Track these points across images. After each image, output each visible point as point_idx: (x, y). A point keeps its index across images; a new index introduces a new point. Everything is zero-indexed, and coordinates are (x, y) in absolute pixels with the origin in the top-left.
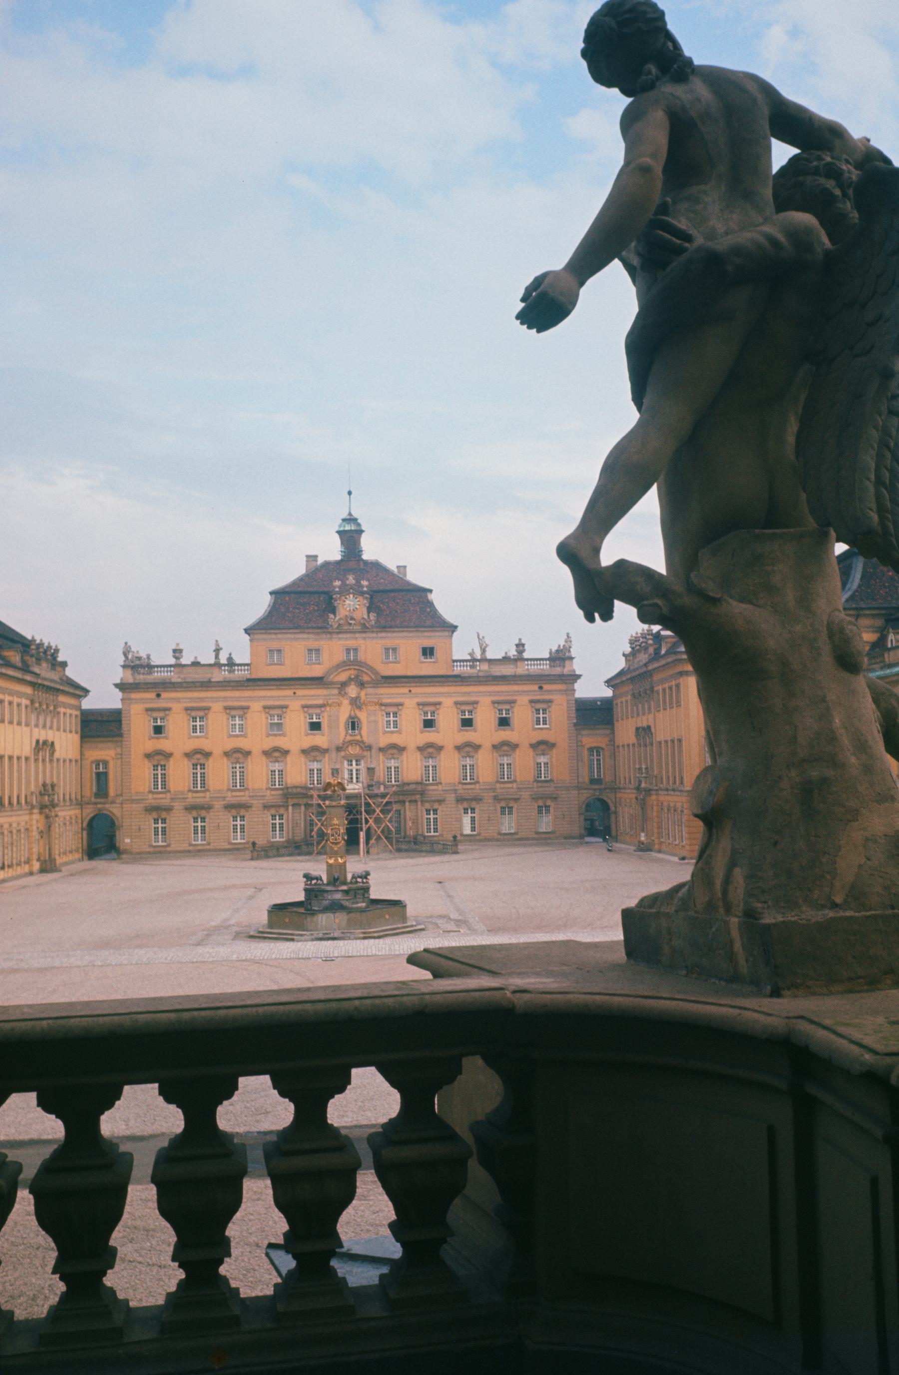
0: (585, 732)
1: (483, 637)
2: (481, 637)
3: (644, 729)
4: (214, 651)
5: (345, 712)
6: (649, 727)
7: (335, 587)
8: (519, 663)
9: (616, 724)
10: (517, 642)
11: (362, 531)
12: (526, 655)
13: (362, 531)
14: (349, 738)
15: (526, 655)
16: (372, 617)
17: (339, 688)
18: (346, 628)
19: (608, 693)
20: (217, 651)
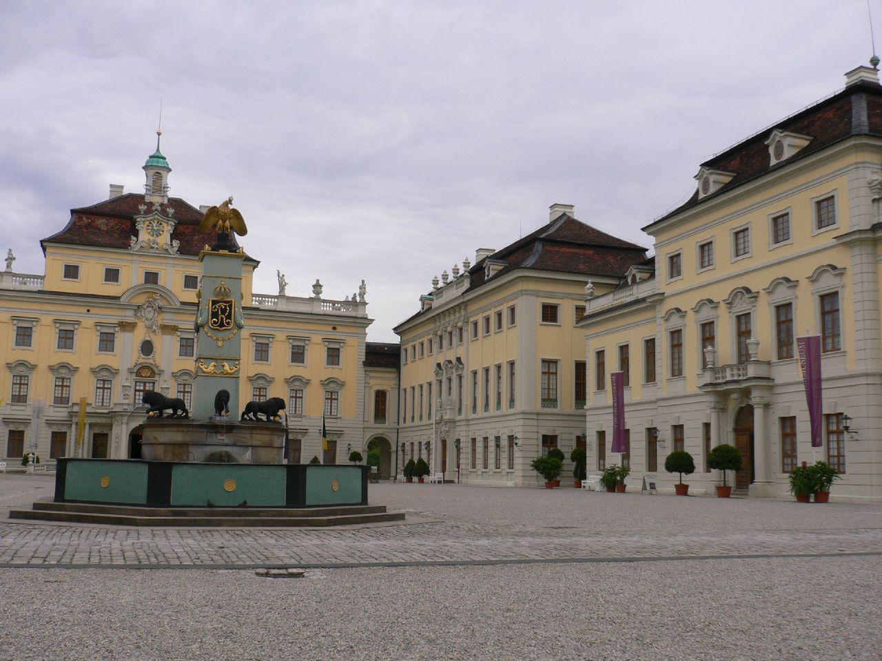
0: (372, 374)
1: (283, 276)
3: (450, 362)
4: (6, 260)
5: (140, 335)
6: (459, 359)
8: (316, 303)
9: (403, 368)
10: (315, 283)
11: (170, 170)
12: (322, 296)
13: (170, 170)
14: (141, 361)
15: (322, 296)
16: (176, 243)
17: (135, 310)
18: (149, 251)
19: (395, 339)
20: (10, 259)
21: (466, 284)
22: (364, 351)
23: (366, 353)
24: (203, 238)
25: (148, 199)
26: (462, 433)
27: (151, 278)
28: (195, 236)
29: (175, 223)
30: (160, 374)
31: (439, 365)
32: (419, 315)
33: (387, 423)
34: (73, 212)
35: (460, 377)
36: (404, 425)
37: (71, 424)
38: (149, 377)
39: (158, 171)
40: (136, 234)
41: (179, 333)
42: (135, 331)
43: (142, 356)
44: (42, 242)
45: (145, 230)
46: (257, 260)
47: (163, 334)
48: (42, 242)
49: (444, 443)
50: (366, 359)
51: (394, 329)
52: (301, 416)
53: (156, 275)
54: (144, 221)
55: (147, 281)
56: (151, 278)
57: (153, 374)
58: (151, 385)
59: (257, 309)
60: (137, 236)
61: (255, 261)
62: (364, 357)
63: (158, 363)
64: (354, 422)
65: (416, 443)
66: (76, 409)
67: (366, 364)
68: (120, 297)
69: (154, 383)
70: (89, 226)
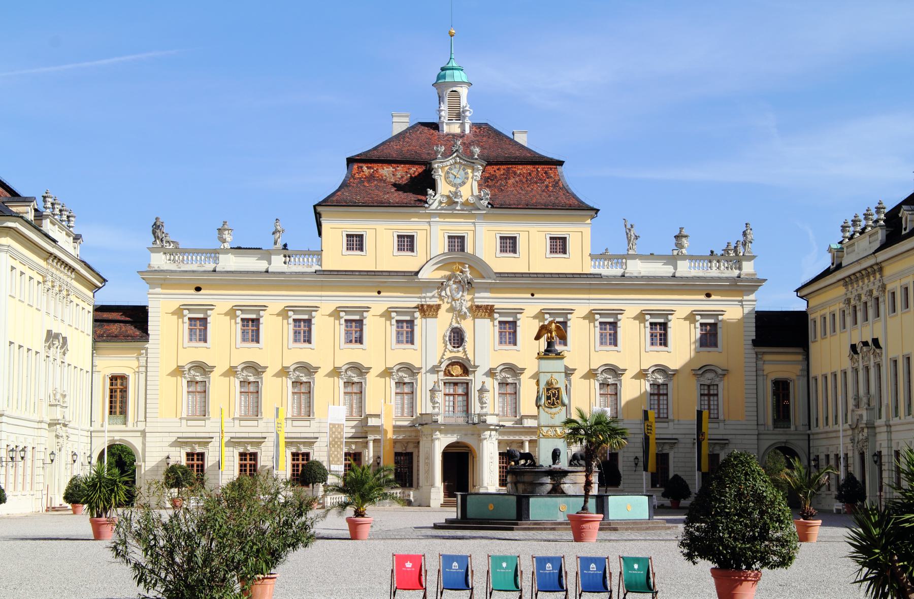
0: (767, 357)
1: (632, 226)
2: (628, 226)
3: (865, 344)
7: (437, 152)
9: (814, 348)
10: (677, 233)
14: (448, 355)
19: (800, 305)
21: (881, 235)
22: (754, 325)
23: (756, 327)
24: (521, 181)
25: (446, 129)
26: (882, 443)
27: (457, 242)
28: (509, 178)
29: (482, 165)
30: (474, 372)
31: (853, 348)
32: (827, 273)
33: (793, 428)
34: (350, 161)
35: (879, 366)
36: (827, 429)
37: (367, 443)
38: (461, 375)
39: (454, 89)
40: (433, 185)
41: (496, 316)
42: (438, 316)
43: (450, 347)
44: (315, 207)
45: (443, 178)
46: (596, 207)
47: (474, 318)
48: (315, 207)
49: (862, 455)
50: (756, 336)
51: (797, 291)
52: (666, 419)
53: (462, 238)
54: (442, 168)
55: (451, 249)
56: (457, 242)
57: (466, 371)
58: (465, 386)
59: (598, 276)
60: (434, 188)
61: (592, 209)
62: (754, 334)
63: (471, 357)
64: (744, 427)
65: (832, 456)
66: (372, 422)
67: (756, 343)
68: (417, 273)
69: (467, 384)
70: (371, 178)
